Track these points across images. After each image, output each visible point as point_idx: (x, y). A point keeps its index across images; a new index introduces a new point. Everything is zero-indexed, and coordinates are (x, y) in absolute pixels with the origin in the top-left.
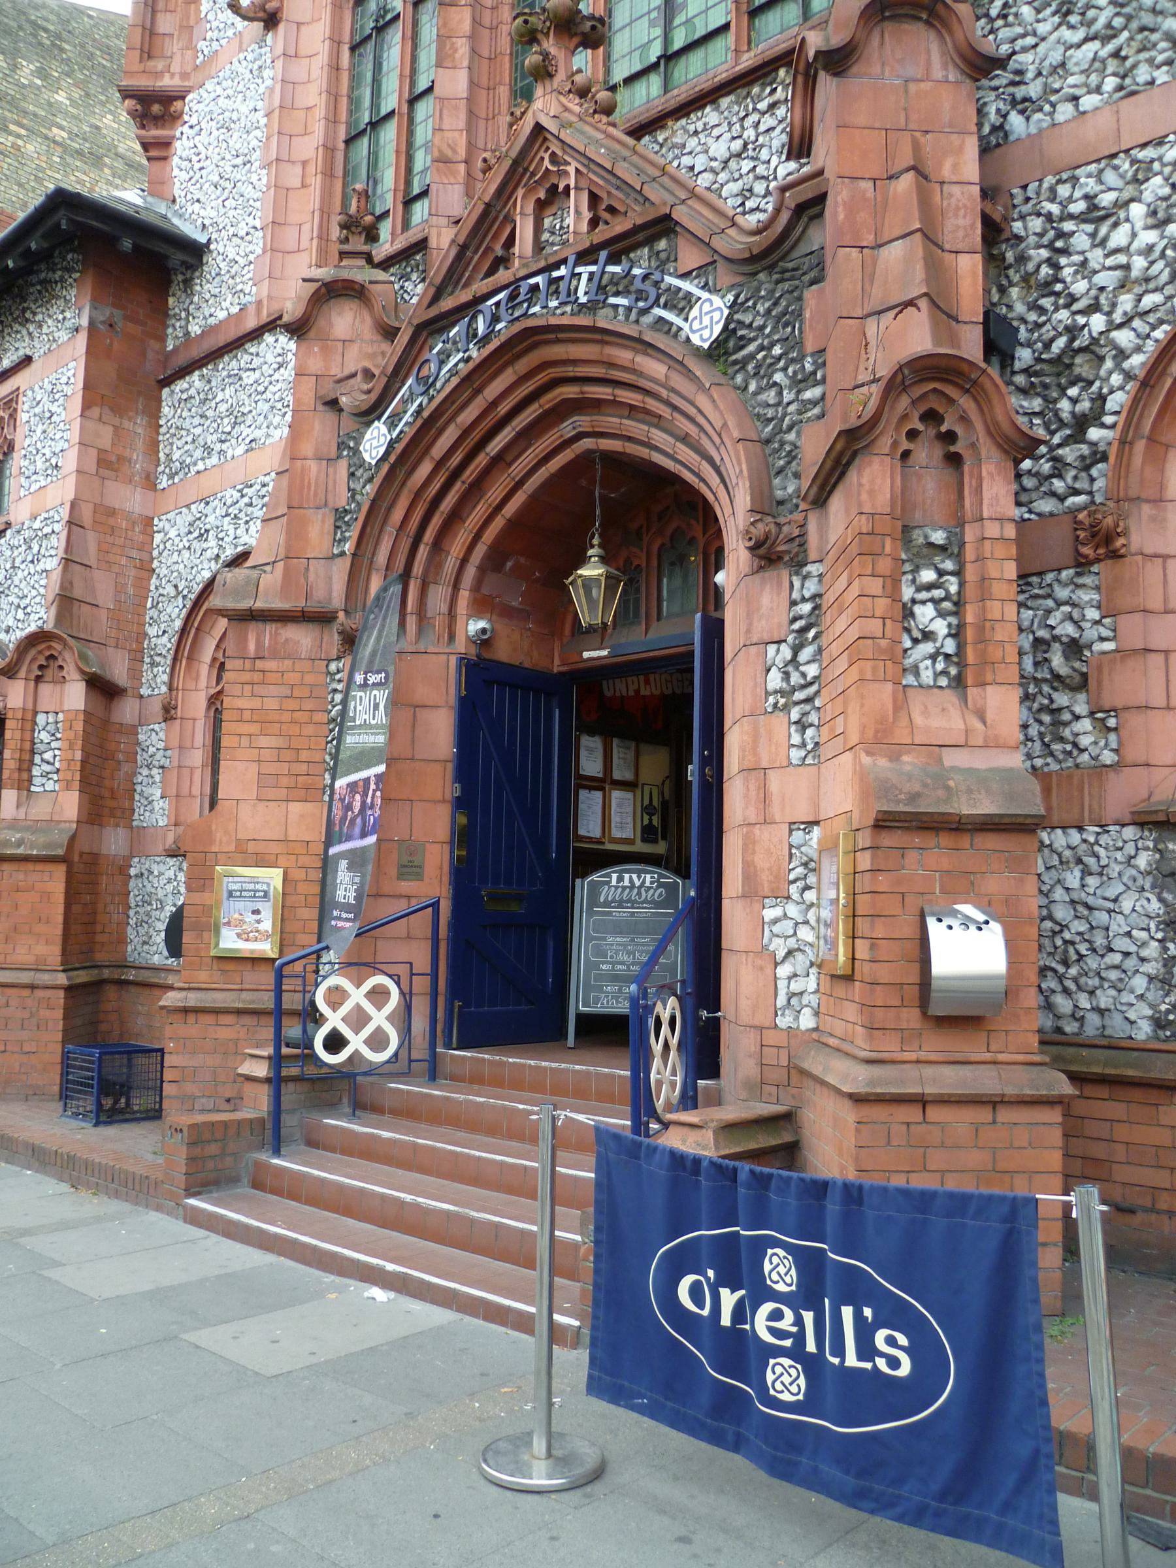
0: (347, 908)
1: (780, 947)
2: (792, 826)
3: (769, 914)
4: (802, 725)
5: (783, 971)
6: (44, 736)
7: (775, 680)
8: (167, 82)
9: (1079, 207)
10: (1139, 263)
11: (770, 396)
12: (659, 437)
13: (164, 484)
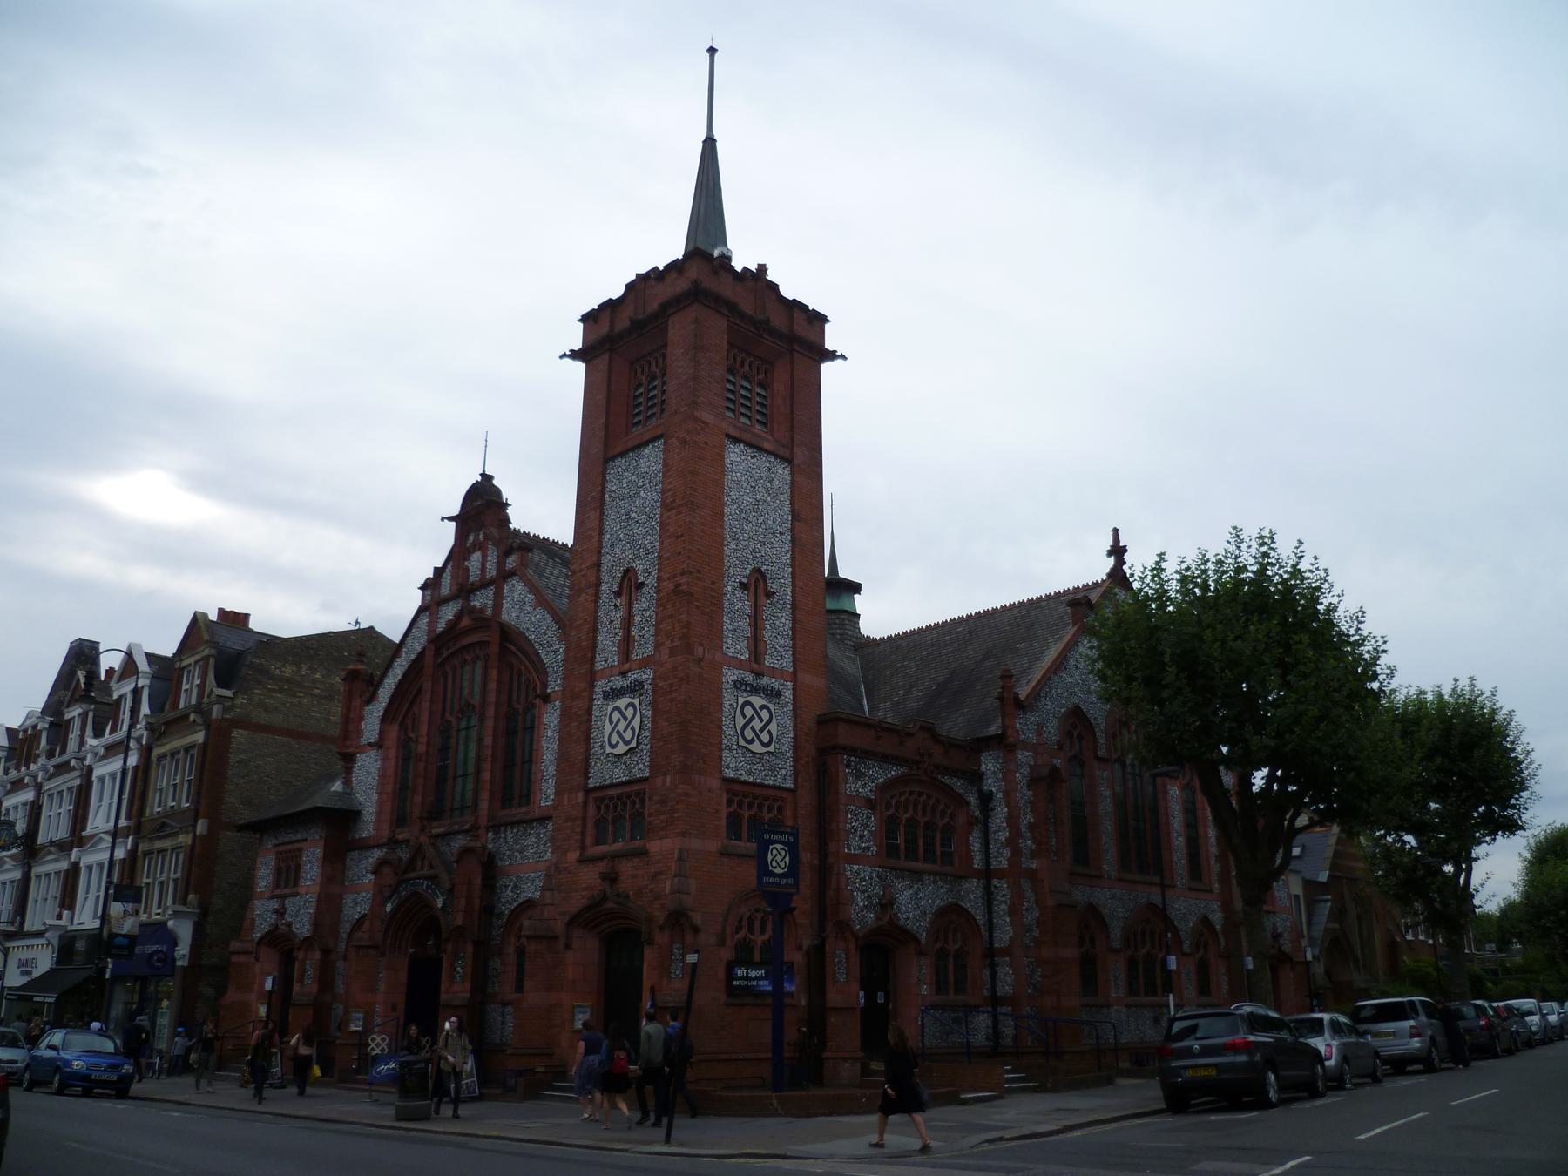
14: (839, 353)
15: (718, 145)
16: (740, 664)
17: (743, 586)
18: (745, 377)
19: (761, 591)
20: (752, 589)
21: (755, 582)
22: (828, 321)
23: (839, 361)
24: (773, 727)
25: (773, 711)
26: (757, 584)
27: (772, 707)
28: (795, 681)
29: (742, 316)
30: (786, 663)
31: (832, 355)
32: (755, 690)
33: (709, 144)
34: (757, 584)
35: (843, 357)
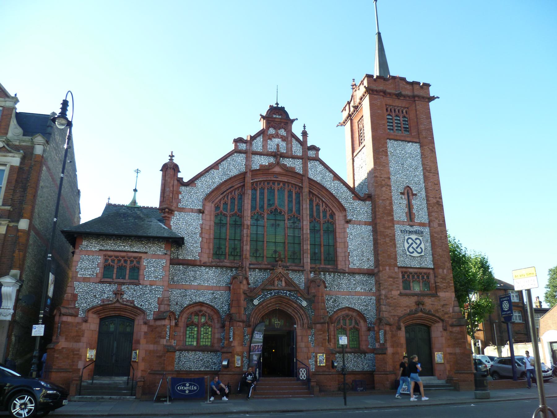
0: (255, 360)
1: (311, 364)
2: (312, 353)
3: (310, 361)
4: (313, 344)
5: (311, 366)
6: (167, 330)
7: (310, 339)
8: (173, 208)
9: (326, 299)
10: (331, 306)
11: (309, 312)
12: (290, 310)
13: (172, 283)
14: (436, 96)
15: (381, 34)
16: (403, 223)
17: (402, 193)
18: (397, 116)
19: (410, 194)
20: (406, 194)
21: (408, 191)
22: (431, 85)
23: (437, 99)
24: (422, 246)
25: (421, 240)
26: (408, 193)
27: (421, 238)
28: (429, 226)
29: (390, 94)
30: (425, 220)
31: (433, 98)
32: (411, 232)
33: (379, 34)
34: (408, 193)
35: (438, 98)
